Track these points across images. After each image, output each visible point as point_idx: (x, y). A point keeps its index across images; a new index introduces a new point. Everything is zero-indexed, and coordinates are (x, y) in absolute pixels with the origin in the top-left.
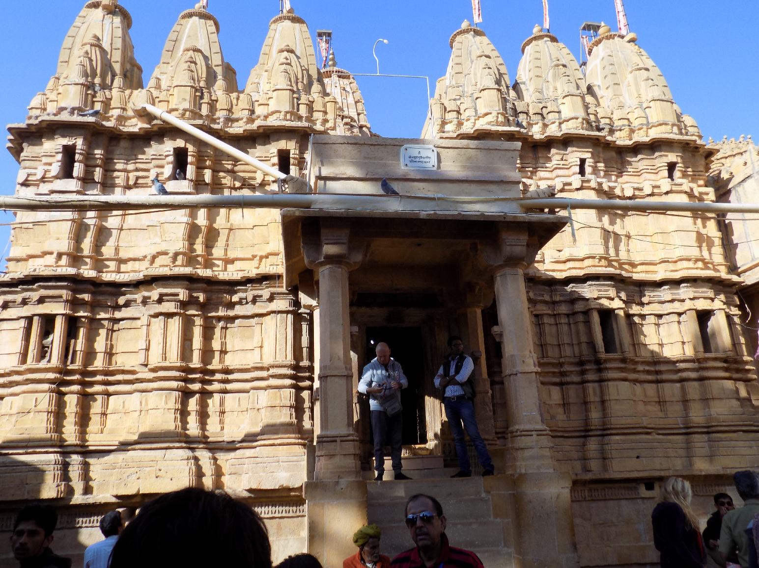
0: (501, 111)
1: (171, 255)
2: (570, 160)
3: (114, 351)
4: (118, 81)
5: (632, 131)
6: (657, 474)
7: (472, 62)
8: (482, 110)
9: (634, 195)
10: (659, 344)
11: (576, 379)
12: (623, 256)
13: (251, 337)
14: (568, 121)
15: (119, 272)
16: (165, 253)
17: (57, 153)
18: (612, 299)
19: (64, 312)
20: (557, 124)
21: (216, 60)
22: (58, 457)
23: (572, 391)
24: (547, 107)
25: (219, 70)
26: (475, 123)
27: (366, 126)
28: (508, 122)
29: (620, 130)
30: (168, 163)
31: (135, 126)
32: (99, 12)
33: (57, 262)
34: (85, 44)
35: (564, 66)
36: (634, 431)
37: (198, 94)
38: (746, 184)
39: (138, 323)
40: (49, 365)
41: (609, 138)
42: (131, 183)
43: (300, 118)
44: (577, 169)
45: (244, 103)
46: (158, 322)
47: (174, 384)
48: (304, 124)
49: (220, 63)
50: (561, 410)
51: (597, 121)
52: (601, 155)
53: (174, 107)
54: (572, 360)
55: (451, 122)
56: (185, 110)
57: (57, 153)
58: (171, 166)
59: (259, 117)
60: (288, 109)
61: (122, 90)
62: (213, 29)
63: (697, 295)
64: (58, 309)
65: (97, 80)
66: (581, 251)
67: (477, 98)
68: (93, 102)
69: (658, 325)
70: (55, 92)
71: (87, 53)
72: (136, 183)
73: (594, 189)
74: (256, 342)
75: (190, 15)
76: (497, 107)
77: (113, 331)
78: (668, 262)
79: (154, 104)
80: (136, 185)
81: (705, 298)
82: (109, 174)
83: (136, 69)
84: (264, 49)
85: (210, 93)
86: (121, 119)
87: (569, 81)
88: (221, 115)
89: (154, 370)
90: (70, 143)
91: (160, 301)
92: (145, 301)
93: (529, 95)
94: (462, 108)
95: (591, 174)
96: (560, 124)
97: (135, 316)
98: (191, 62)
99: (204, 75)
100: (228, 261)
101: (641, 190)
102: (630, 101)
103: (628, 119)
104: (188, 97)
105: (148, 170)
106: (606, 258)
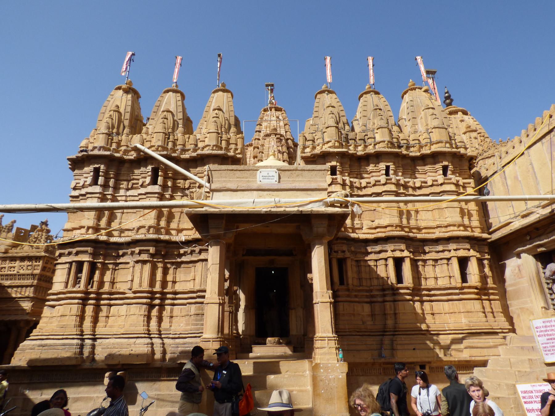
0: (337, 139)
1: (147, 228)
2: (380, 167)
3: (115, 281)
4: (127, 130)
5: (421, 147)
6: (427, 360)
7: (324, 110)
8: (326, 139)
9: (421, 186)
10: (435, 278)
11: (380, 299)
12: (413, 223)
13: (190, 273)
14: (379, 143)
15: (120, 237)
16: (144, 227)
17: (91, 172)
18: (403, 251)
19: (88, 259)
20: (373, 145)
21: (180, 116)
22: (79, 342)
23: (377, 307)
24: (367, 135)
25: (181, 122)
26: (322, 147)
27: (290, 139)
28: (341, 146)
29: (413, 147)
30: (149, 176)
31: (132, 155)
32: (121, 92)
33: (86, 232)
34: (110, 111)
35: (380, 109)
36: (413, 333)
37: (167, 136)
38: (494, 176)
39: (128, 266)
40: (79, 289)
41: (405, 152)
42: (130, 187)
43: (221, 149)
44: (384, 172)
45: (192, 140)
46: (138, 266)
47: (144, 301)
48: (222, 152)
49: (182, 118)
50: (370, 319)
51: (398, 142)
52: (400, 162)
53: (154, 144)
54: (378, 288)
55: (308, 147)
56: (159, 146)
57: (91, 172)
58: (150, 177)
59: (199, 148)
60: (214, 144)
61: (128, 135)
62: (180, 98)
63: (459, 247)
64: (85, 258)
65: (115, 130)
66: (385, 222)
67: (324, 132)
68: (112, 143)
69: (434, 266)
70: (93, 138)
71: (111, 116)
72: (132, 187)
73: (394, 184)
74: (191, 277)
75: (168, 91)
76: (335, 137)
77: (115, 270)
78: (441, 227)
79: (143, 144)
80: (132, 188)
81: (464, 249)
82: (118, 182)
83: (139, 122)
84: (206, 109)
85: (174, 135)
86: (126, 152)
87: (382, 119)
88: (179, 147)
89: (135, 292)
90: (98, 166)
91: (140, 253)
92: (132, 253)
93: (357, 129)
94: (316, 138)
95: (393, 174)
96: (375, 145)
97: (127, 261)
98: (165, 118)
99: (171, 125)
100: (179, 231)
101: (426, 183)
102: (421, 128)
103: (419, 140)
104: (161, 139)
105: (138, 180)
106: (400, 226)
